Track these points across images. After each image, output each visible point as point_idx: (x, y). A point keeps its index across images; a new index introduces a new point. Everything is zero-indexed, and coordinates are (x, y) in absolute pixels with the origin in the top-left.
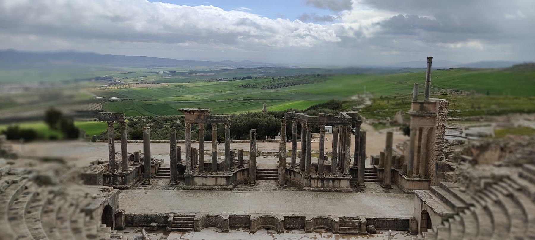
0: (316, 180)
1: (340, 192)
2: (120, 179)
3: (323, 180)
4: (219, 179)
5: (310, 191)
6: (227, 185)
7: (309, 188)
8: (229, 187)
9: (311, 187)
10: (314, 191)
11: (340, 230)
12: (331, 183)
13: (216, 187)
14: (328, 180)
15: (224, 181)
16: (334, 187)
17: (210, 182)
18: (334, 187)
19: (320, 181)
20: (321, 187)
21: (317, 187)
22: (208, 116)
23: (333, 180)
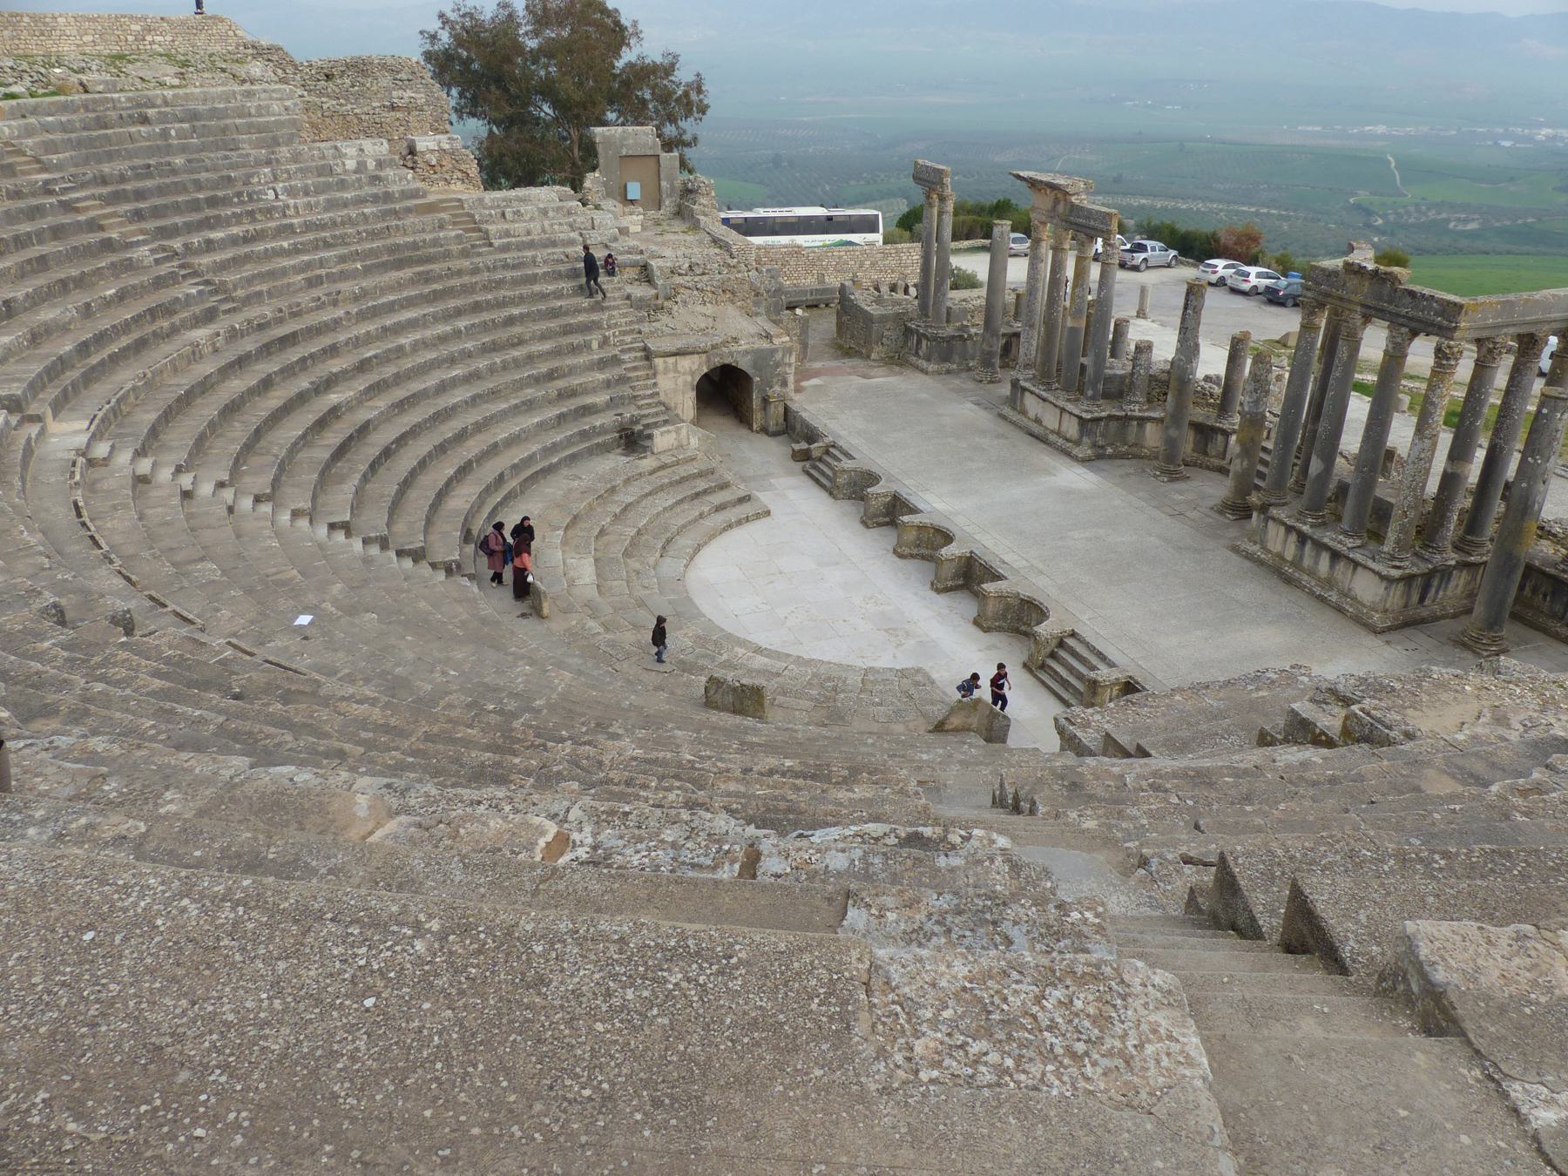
0: (1282, 530)
1: (1340, 610)
2: (924, 342)
3: (1303, 538)
4: (1066, 417)
5: (1249, 557)
6: (1078, 443)
7: (1257, 547)
8: (1076, 451)
9: (1264, 548)
10: (1260, 563)
11: (1043, 666)
12: (1325, 561)
13: (1052, 438)
14: (1320, 546)
15: (1071, 428)
16: (1329, 583)
17: (1051, 420)
18: (1329, 583)
19: (1293, 538)
20: (1292, 564)
21: (1281, 557)
22: (1072, 205)
23: (1336, 556)
